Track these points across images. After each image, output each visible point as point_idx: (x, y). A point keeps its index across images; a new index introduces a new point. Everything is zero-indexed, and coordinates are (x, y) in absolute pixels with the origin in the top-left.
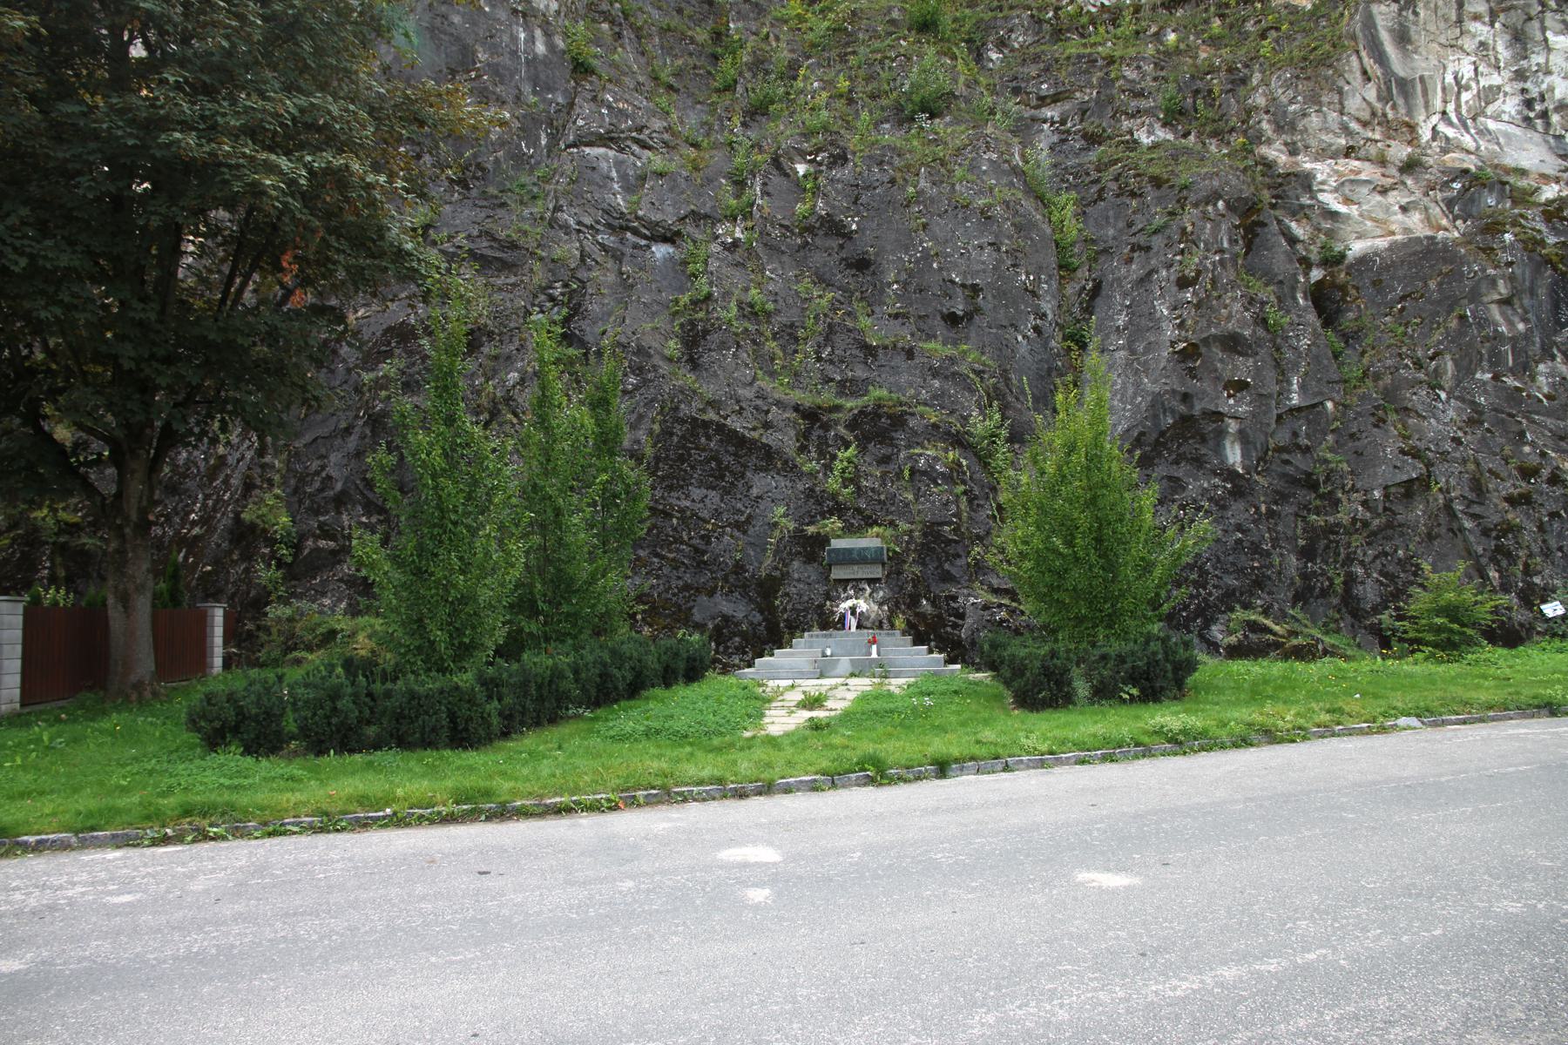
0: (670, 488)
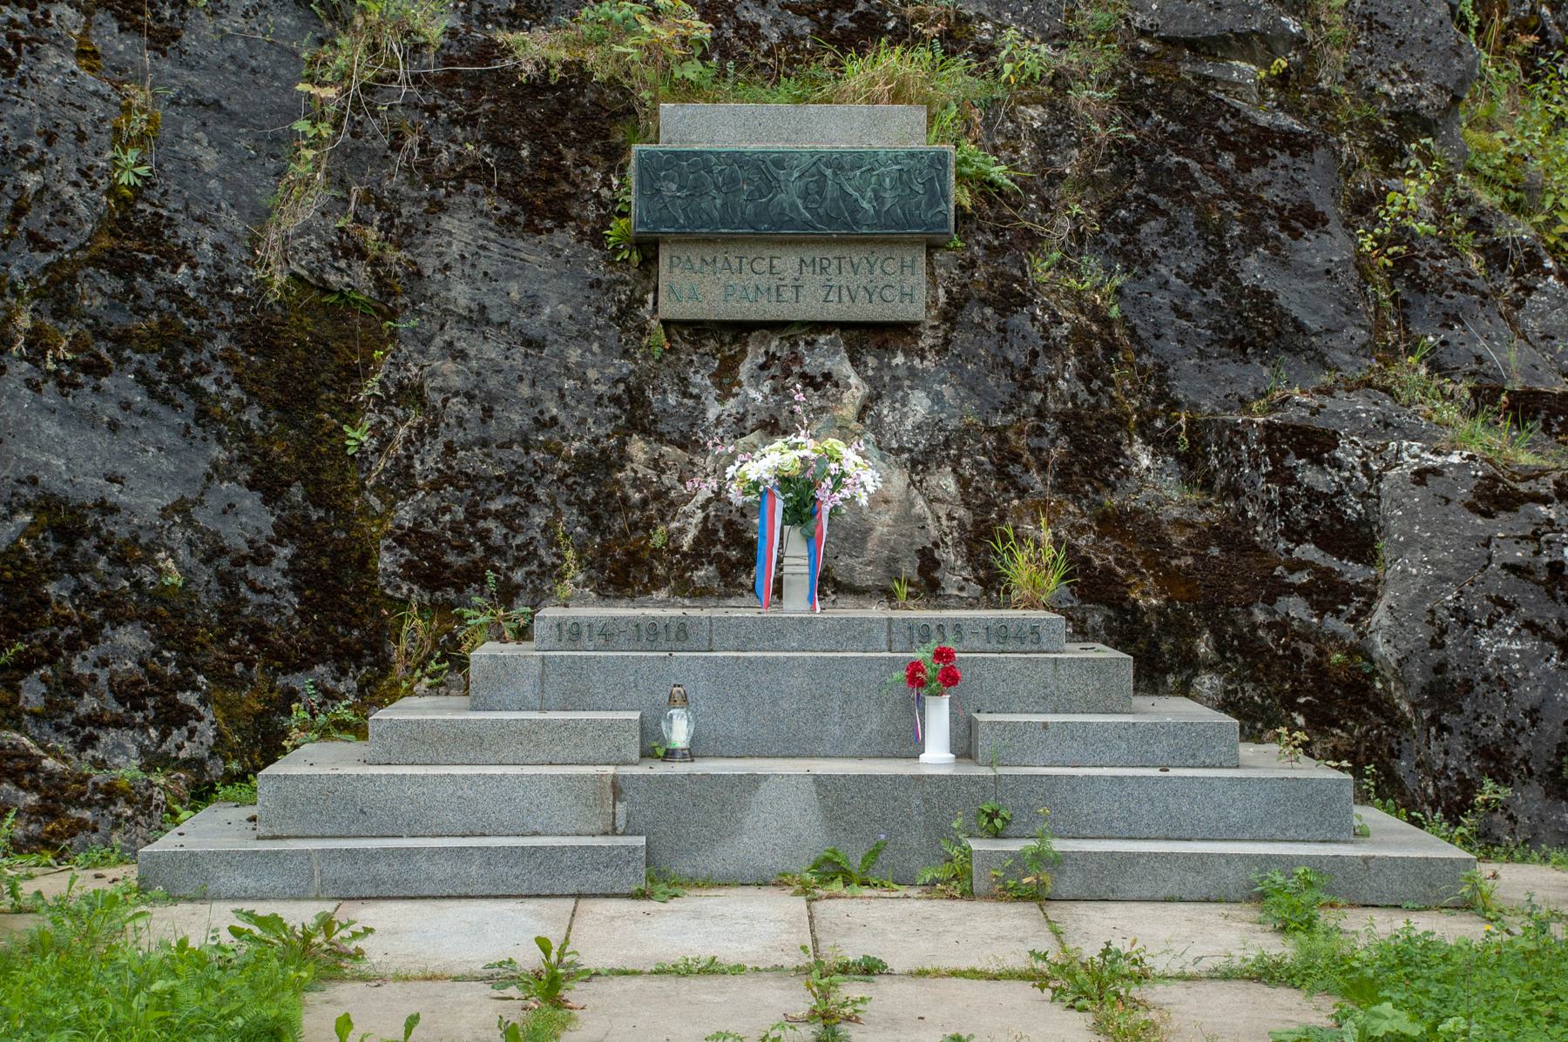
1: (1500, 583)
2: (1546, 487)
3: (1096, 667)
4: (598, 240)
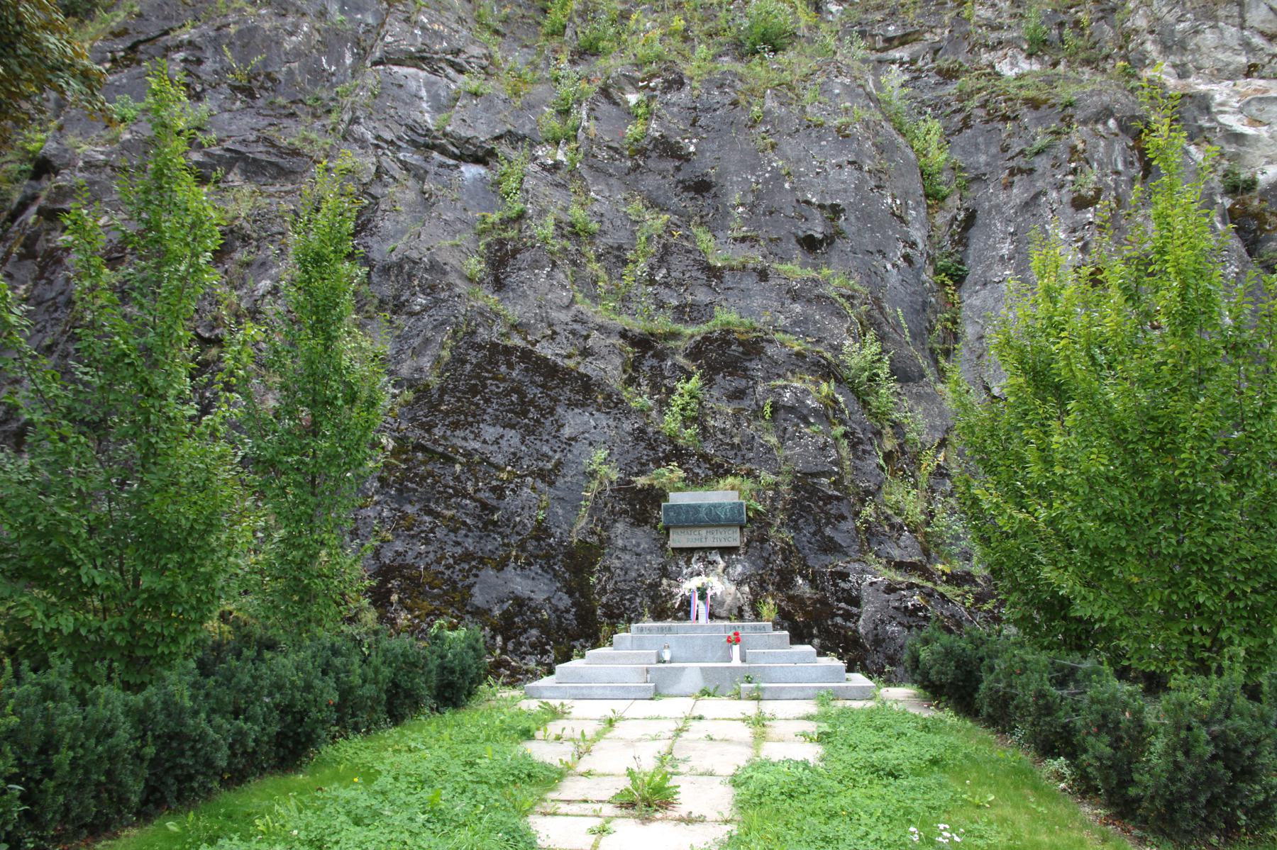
0: (456, 425)
1: (892, 612)
2: (904, 586)
3: (780, 637)
4: (655, 528)
